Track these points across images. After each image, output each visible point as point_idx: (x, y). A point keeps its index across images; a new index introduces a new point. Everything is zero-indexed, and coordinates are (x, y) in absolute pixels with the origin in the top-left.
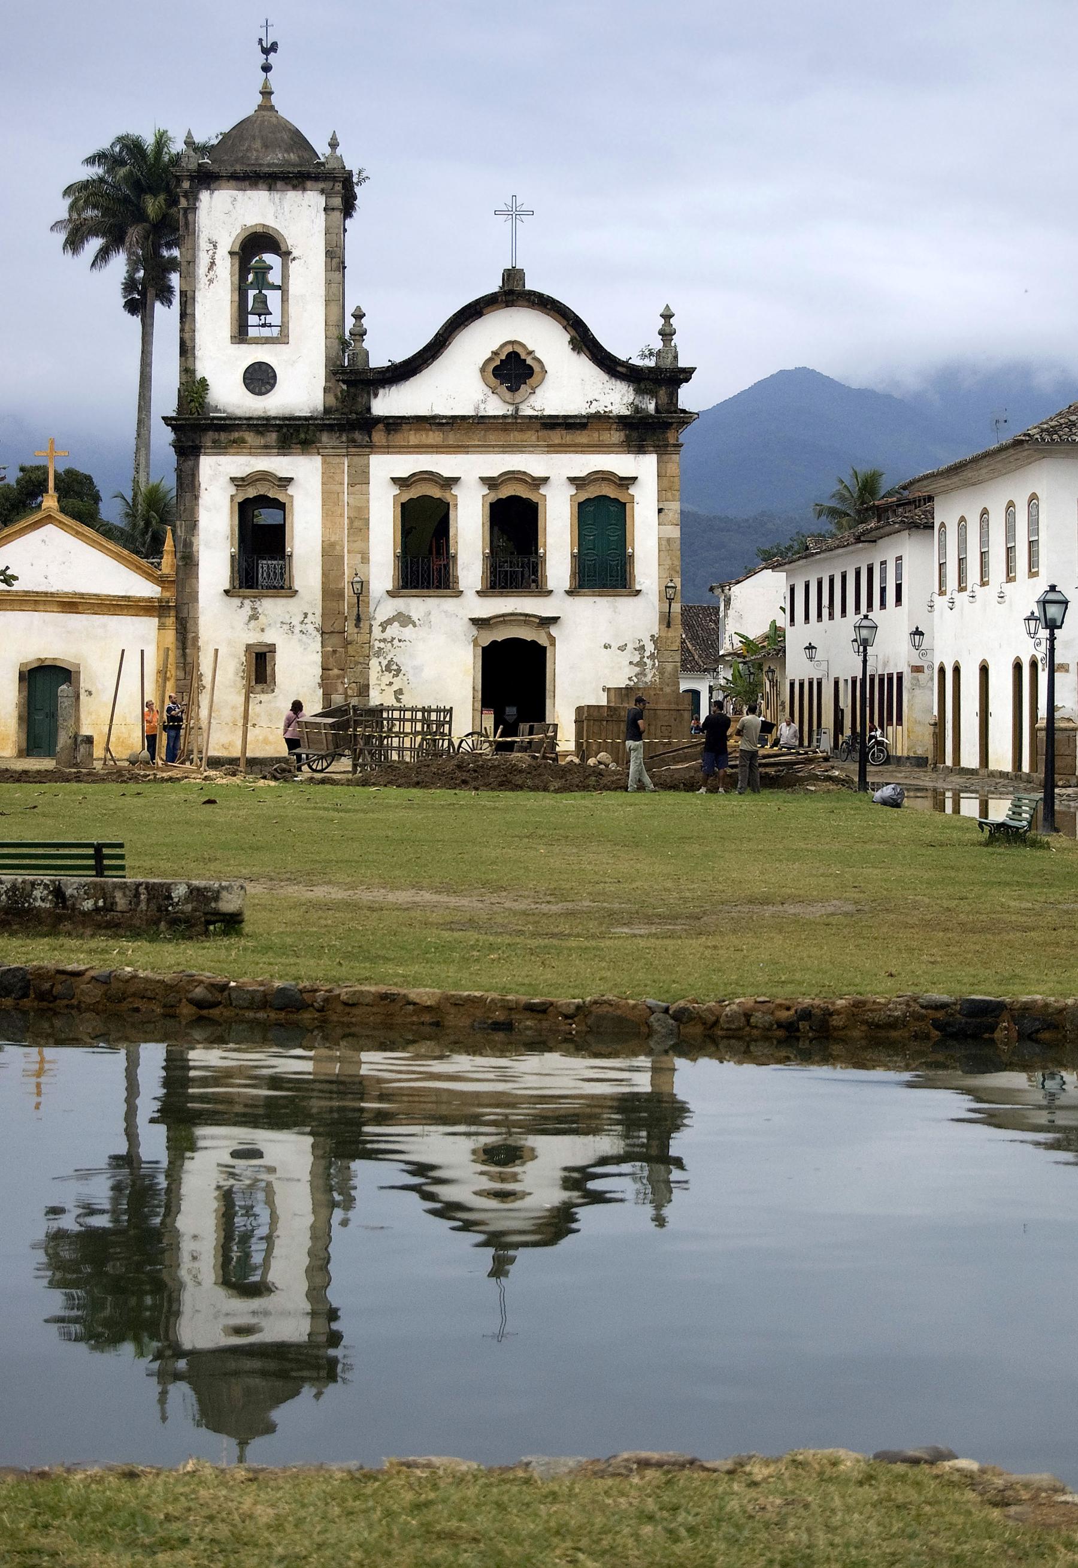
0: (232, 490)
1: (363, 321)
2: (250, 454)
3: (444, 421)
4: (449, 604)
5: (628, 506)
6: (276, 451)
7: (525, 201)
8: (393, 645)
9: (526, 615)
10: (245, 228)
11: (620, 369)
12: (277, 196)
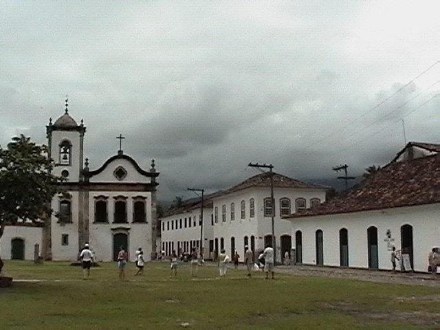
4: (107, 225)
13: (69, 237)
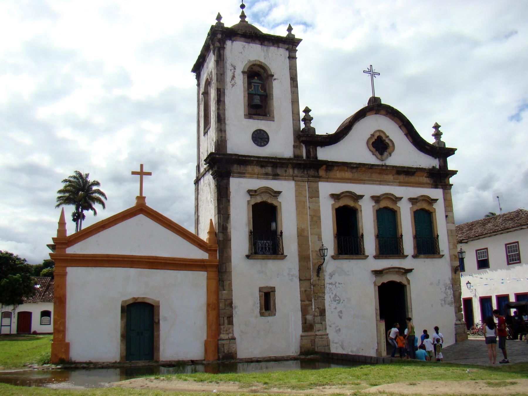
0: (248, 198)
1: (310, 113)
2: (258, 178)
3: (355, 166)
5: (434, 214)
6: (271, 177)
7: (376, 69)
8: (336, 286)
10: (249, 61)
11: (427, 147)
12: (265, 48)
13: (276, 293)
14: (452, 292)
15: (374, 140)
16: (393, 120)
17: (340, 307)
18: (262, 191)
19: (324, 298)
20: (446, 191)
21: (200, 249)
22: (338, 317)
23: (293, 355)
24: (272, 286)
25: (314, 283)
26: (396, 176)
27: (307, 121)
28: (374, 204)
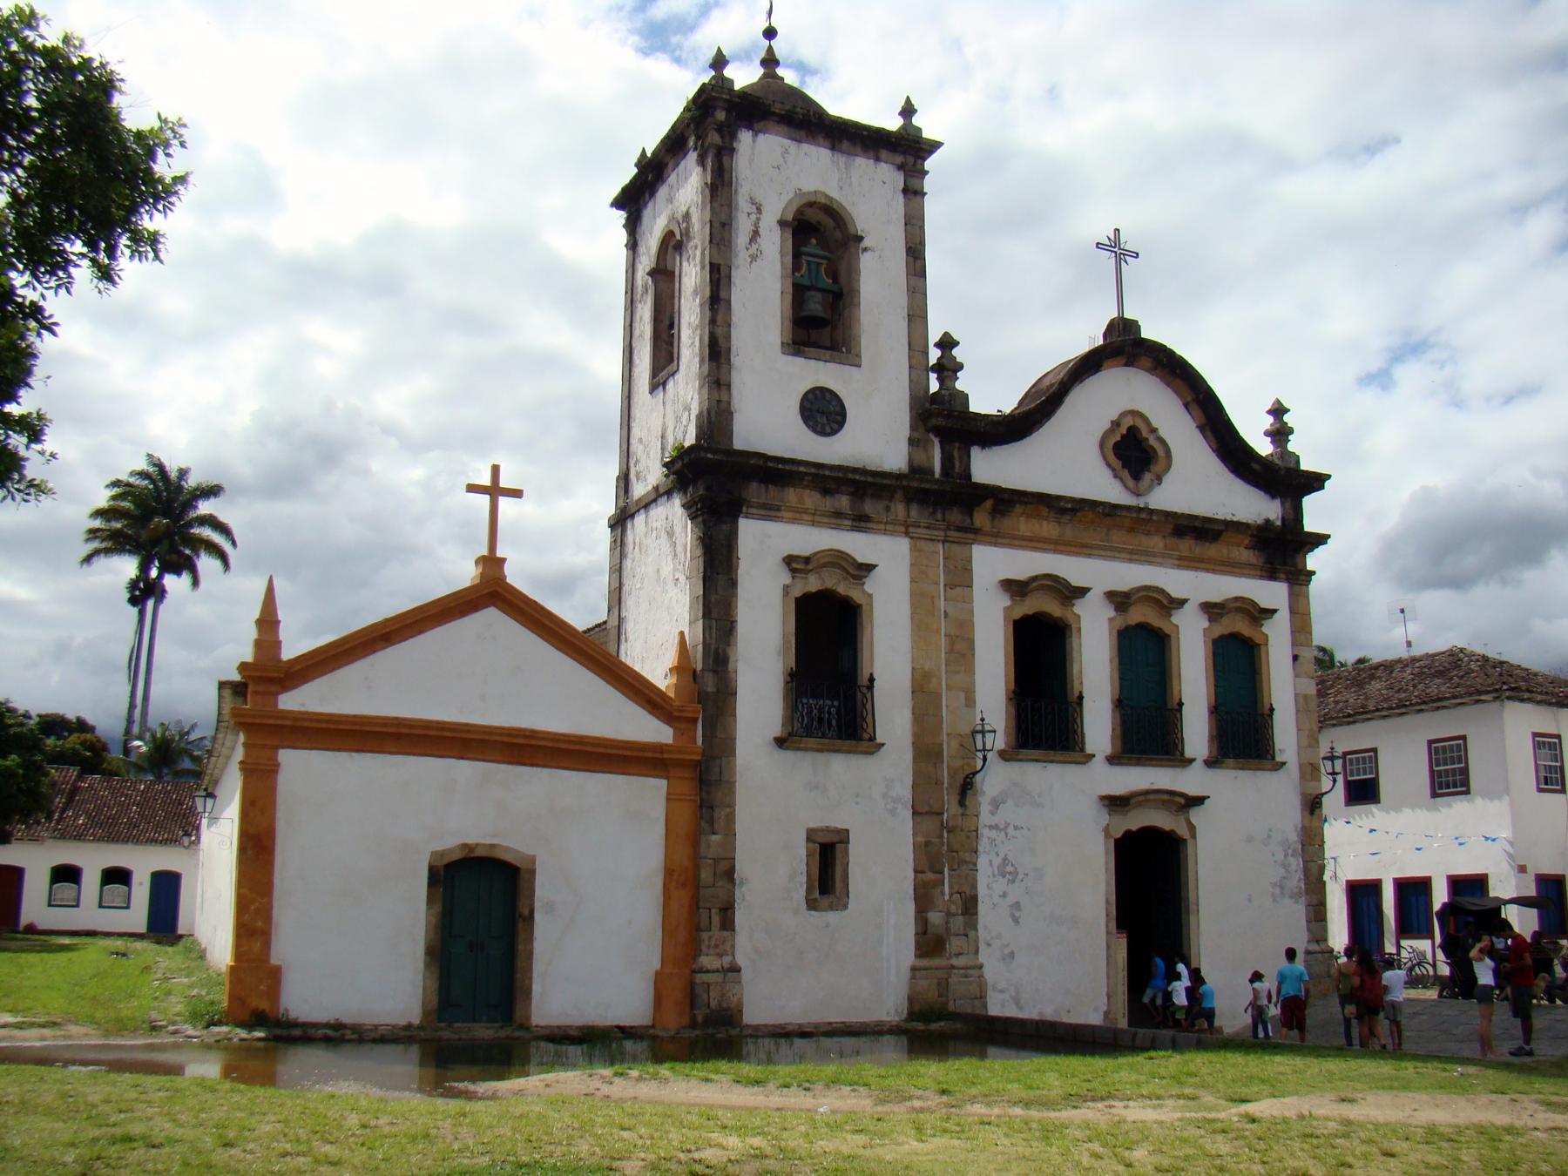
0: (785, 577)
1: (955, 352)
2: (813, 524)
5: (1263, 648)
7: (1128, 242)
9: (1172, 793)
10: (799, 193)
11: (1256, 466)
12: (842, 159)
13: (851, 846)
14: (1302, 866)
15: (1118, 438)
16: (1168, 384)
17: (1015, 893)
18: (826, 560)
19: (976, 865)
20: (1296, 588)
21: (650, 713)
22: (1010, 920)
23: (889, 1019)
24: (841, 826)
25: (950, 825)
26: (1171, 541)
27: (946, 373)
28: (1112, 613)
